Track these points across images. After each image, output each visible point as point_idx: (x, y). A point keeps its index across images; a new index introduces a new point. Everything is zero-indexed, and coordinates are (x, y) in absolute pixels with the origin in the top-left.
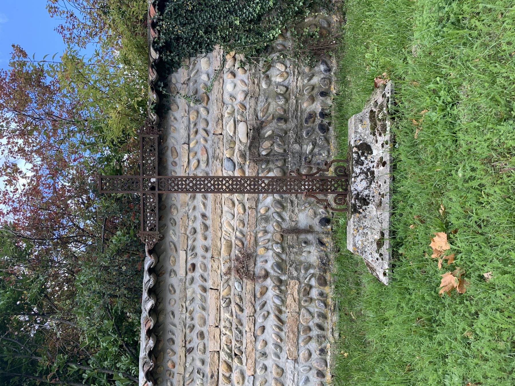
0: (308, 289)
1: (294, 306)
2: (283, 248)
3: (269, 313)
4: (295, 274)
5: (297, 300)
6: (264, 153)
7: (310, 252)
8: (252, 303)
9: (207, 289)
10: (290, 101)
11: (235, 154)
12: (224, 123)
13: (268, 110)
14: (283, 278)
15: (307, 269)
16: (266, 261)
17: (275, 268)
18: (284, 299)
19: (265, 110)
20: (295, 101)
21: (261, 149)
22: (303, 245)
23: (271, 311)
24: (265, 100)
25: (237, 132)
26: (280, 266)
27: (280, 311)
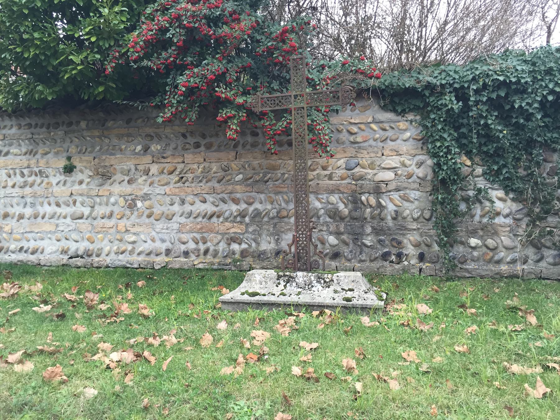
0: (238, 241)
1: (222, 228)
2: (273, 218)
3: (217, 206)
4: (250, 230)
5: (228, 231)
6: (363, 198)
7: (270, 243)
8: (224, 191)
9: (236, 149)
10: (415, 224)
11: (362, 170)
12: (394, 157)
13: (406, 201)
14: (247, 219)
15: (255, 240)
16: (261, 203)
17: (256, 212)
18: (229, 220)
19: (406, 198)
20: (414, 227)
21: (367, 195)
22: (276, 237)
23: (219, 208)
24: (416, 198)
25: (385, 170)
26: (257, 214)
27: (218, 217)
